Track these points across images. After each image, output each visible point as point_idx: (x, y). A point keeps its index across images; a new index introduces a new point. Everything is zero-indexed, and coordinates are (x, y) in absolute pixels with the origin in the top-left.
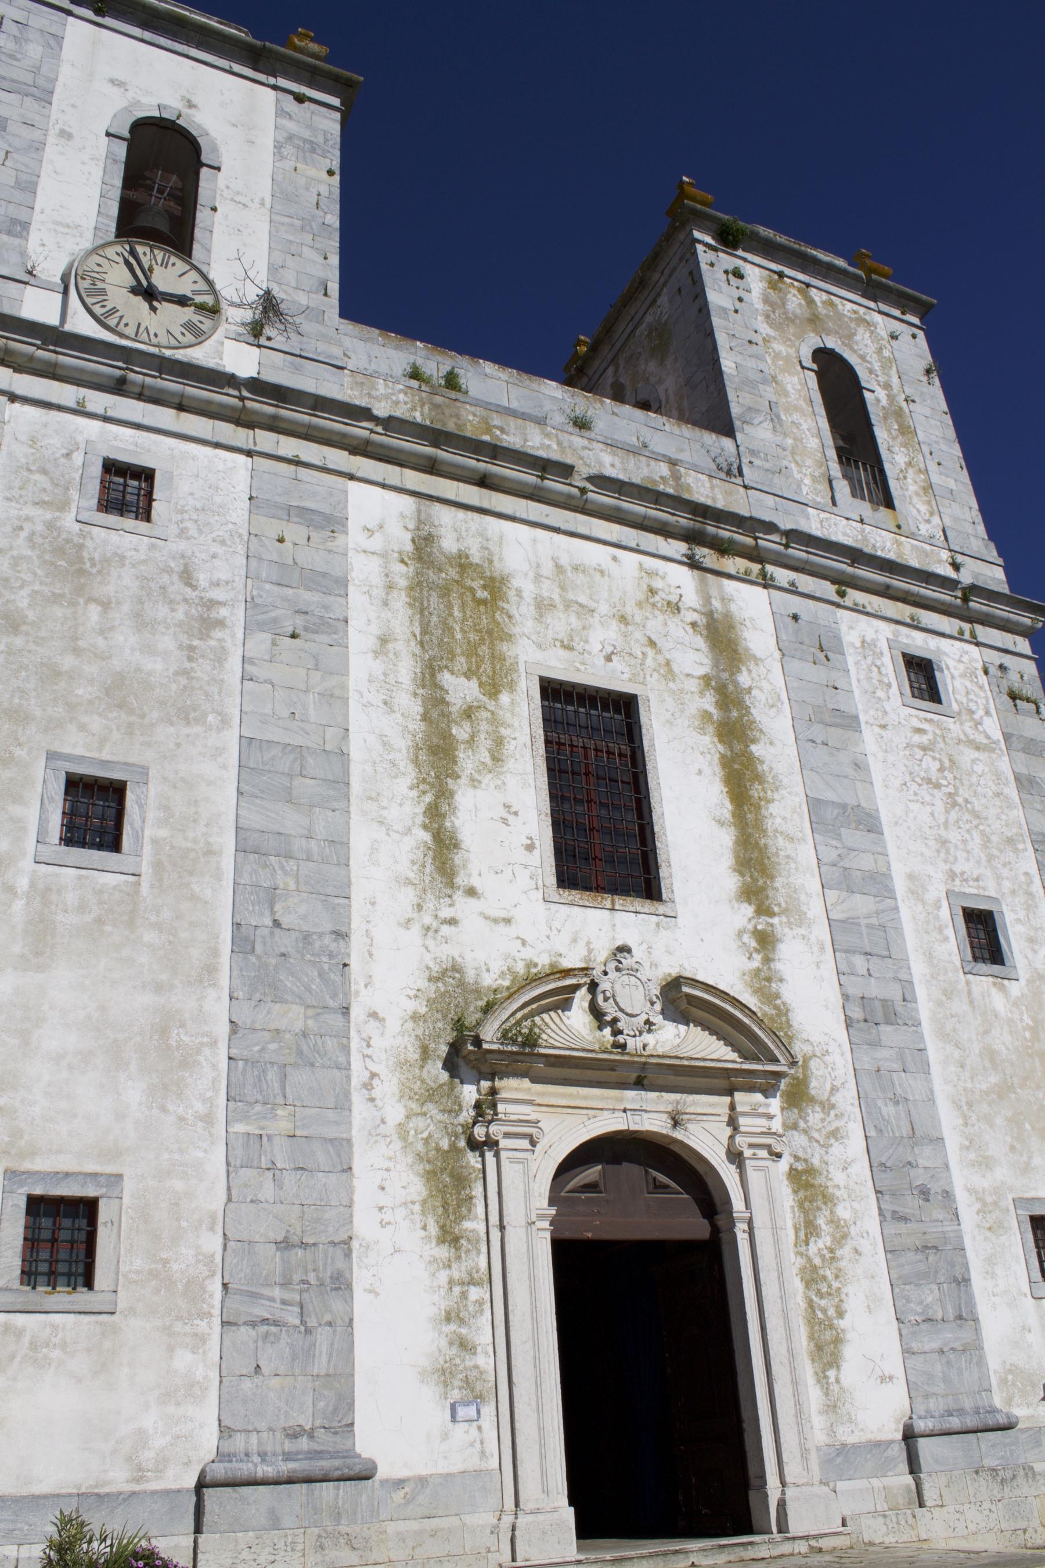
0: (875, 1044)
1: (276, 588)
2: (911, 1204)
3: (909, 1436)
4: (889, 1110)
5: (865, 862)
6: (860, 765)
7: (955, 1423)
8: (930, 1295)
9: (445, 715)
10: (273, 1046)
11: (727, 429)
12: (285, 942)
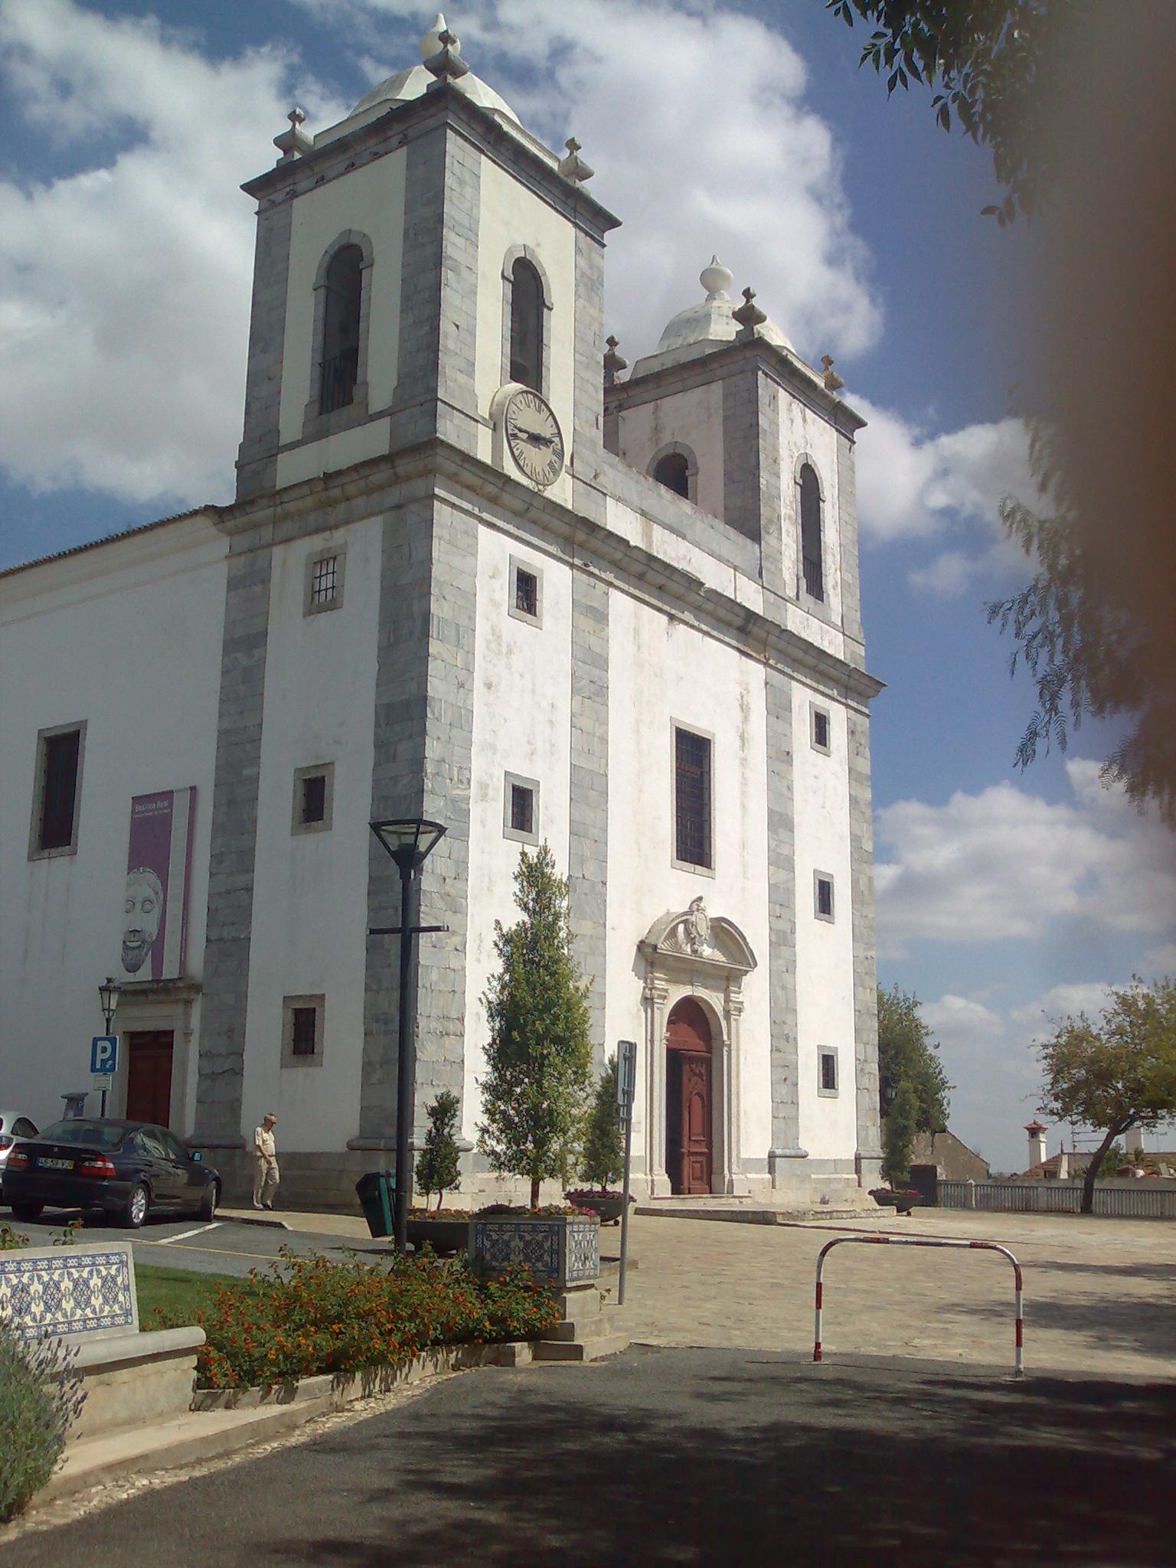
0: (779, 957)
2: (782, 1044)
3: (772, 1156)
4: (780, 992)
5: (785, 850)
6: (790, 788)
11: (756, 536)
12: (587, 885)
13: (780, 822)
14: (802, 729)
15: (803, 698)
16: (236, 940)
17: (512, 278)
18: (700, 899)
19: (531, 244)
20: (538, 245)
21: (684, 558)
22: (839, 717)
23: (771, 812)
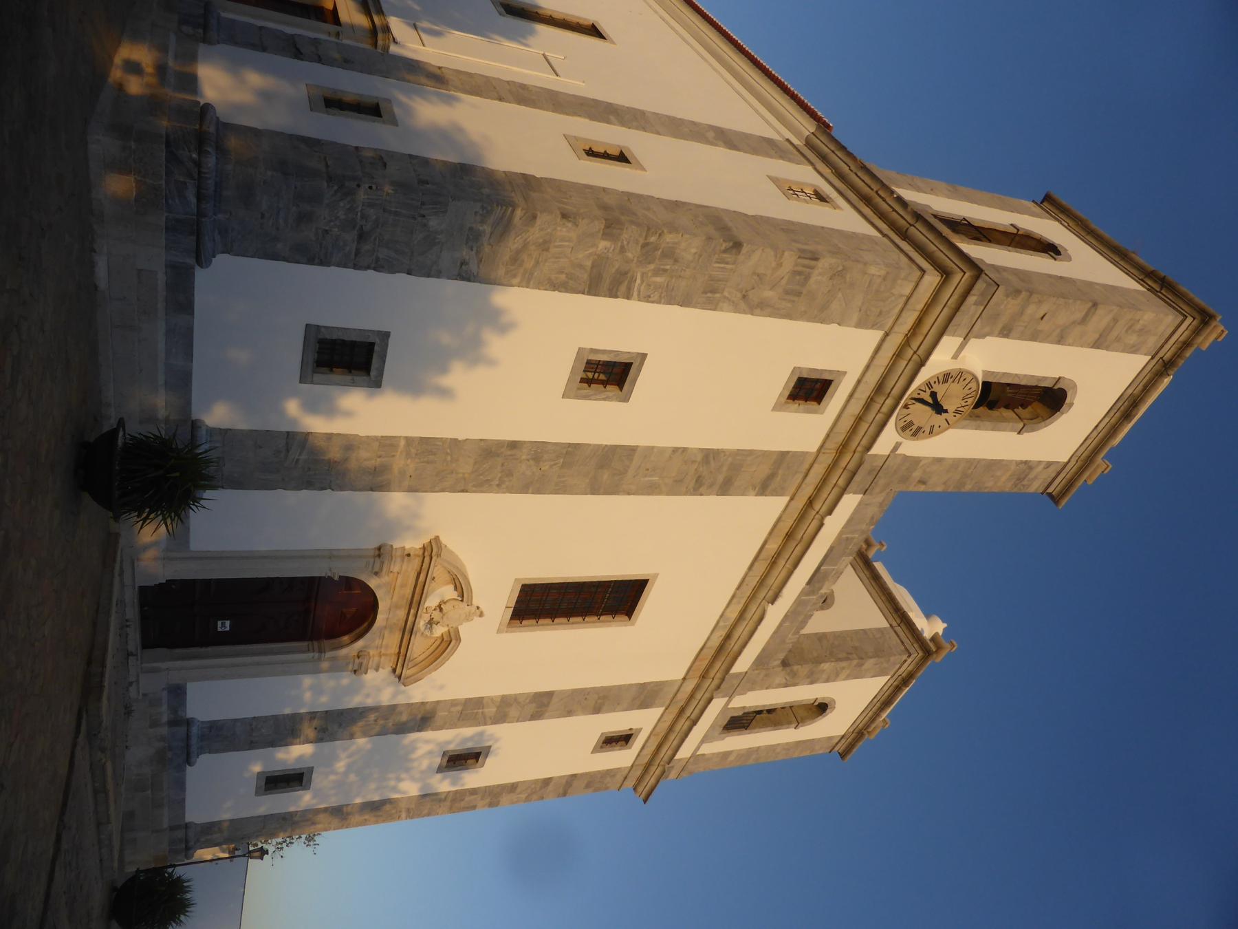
5: (513, 712)
13: (540, 705)
14: (616, 722)
15: (644, 721)
18: (481, 615)
22: (622, 758)
23: (550, 694)
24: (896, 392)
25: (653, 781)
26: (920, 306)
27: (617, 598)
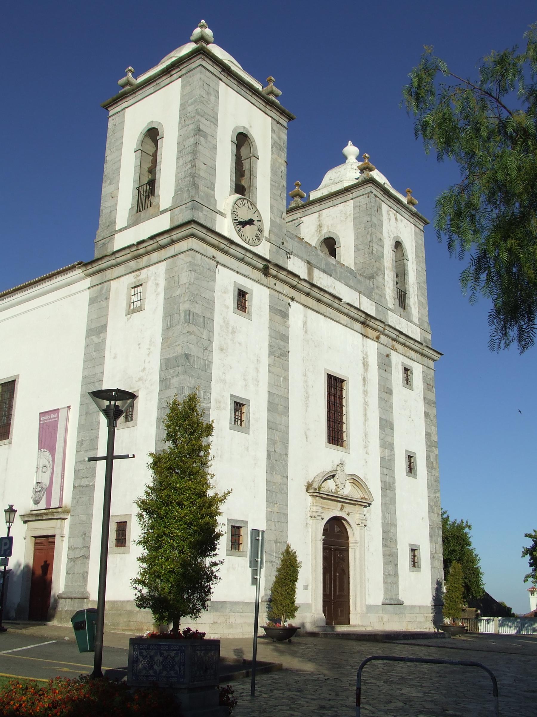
1: (275, 340)
4: (387, 515)
5: (389, 439)
7: (393, 602)
8: (390, 568)
9: (307, 386)
10: (274, 487)
13: (386, 425)
14: (397, 375)
15: (398, 360)
16: (88, 486)
17: (236, 142)
19: (247, 126)
20: (251, 127)
21: (331, 286)
22: (418, 372)
23: (381, 419)
24: (243, 252)
25: (431, 351)
26: (205, 246)
27: (335, 385)
